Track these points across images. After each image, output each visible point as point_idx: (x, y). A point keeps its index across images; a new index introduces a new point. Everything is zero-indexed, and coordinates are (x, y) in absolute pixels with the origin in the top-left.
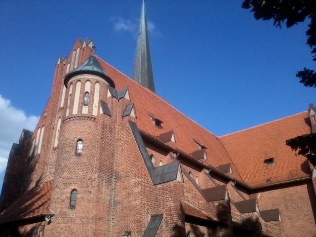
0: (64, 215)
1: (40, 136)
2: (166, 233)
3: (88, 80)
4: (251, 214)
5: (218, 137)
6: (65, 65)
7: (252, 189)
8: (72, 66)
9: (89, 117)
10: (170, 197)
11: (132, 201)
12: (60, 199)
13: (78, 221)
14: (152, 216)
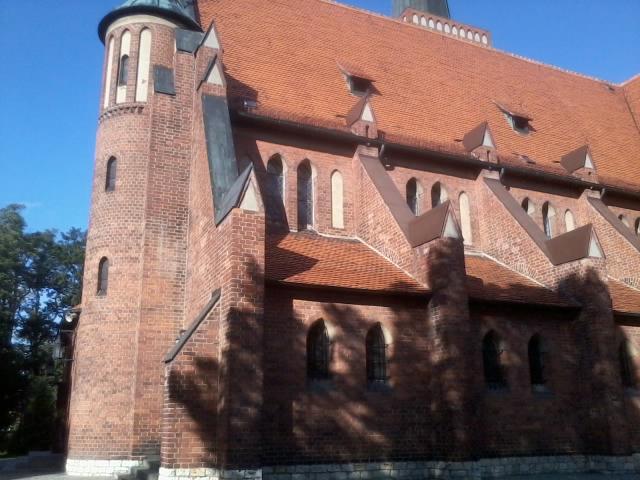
4: (576, 264)
9: (128, 108)
13: (112, 317)
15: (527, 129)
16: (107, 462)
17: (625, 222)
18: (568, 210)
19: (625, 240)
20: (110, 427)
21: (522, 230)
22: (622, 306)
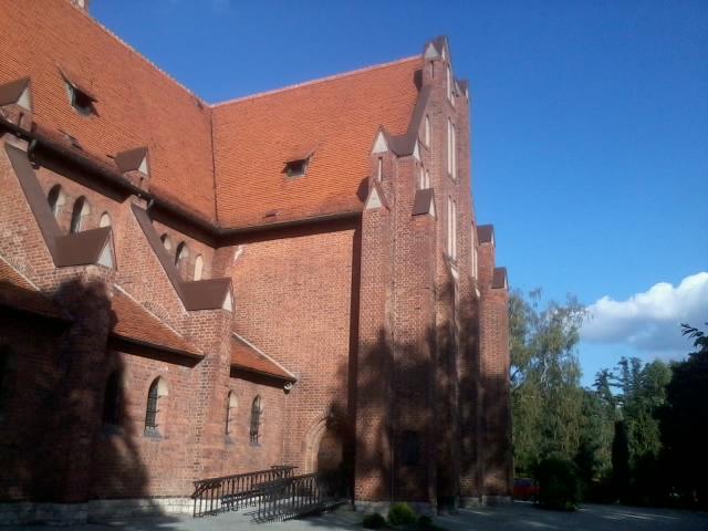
4: (80, 269)
5: (204, 103)
7: (221, 232)
15: (88, 109)
17: (168, 246)
18: (105, 213)
19: (157, 259)
21: (32, 218)
22: (124, 330)
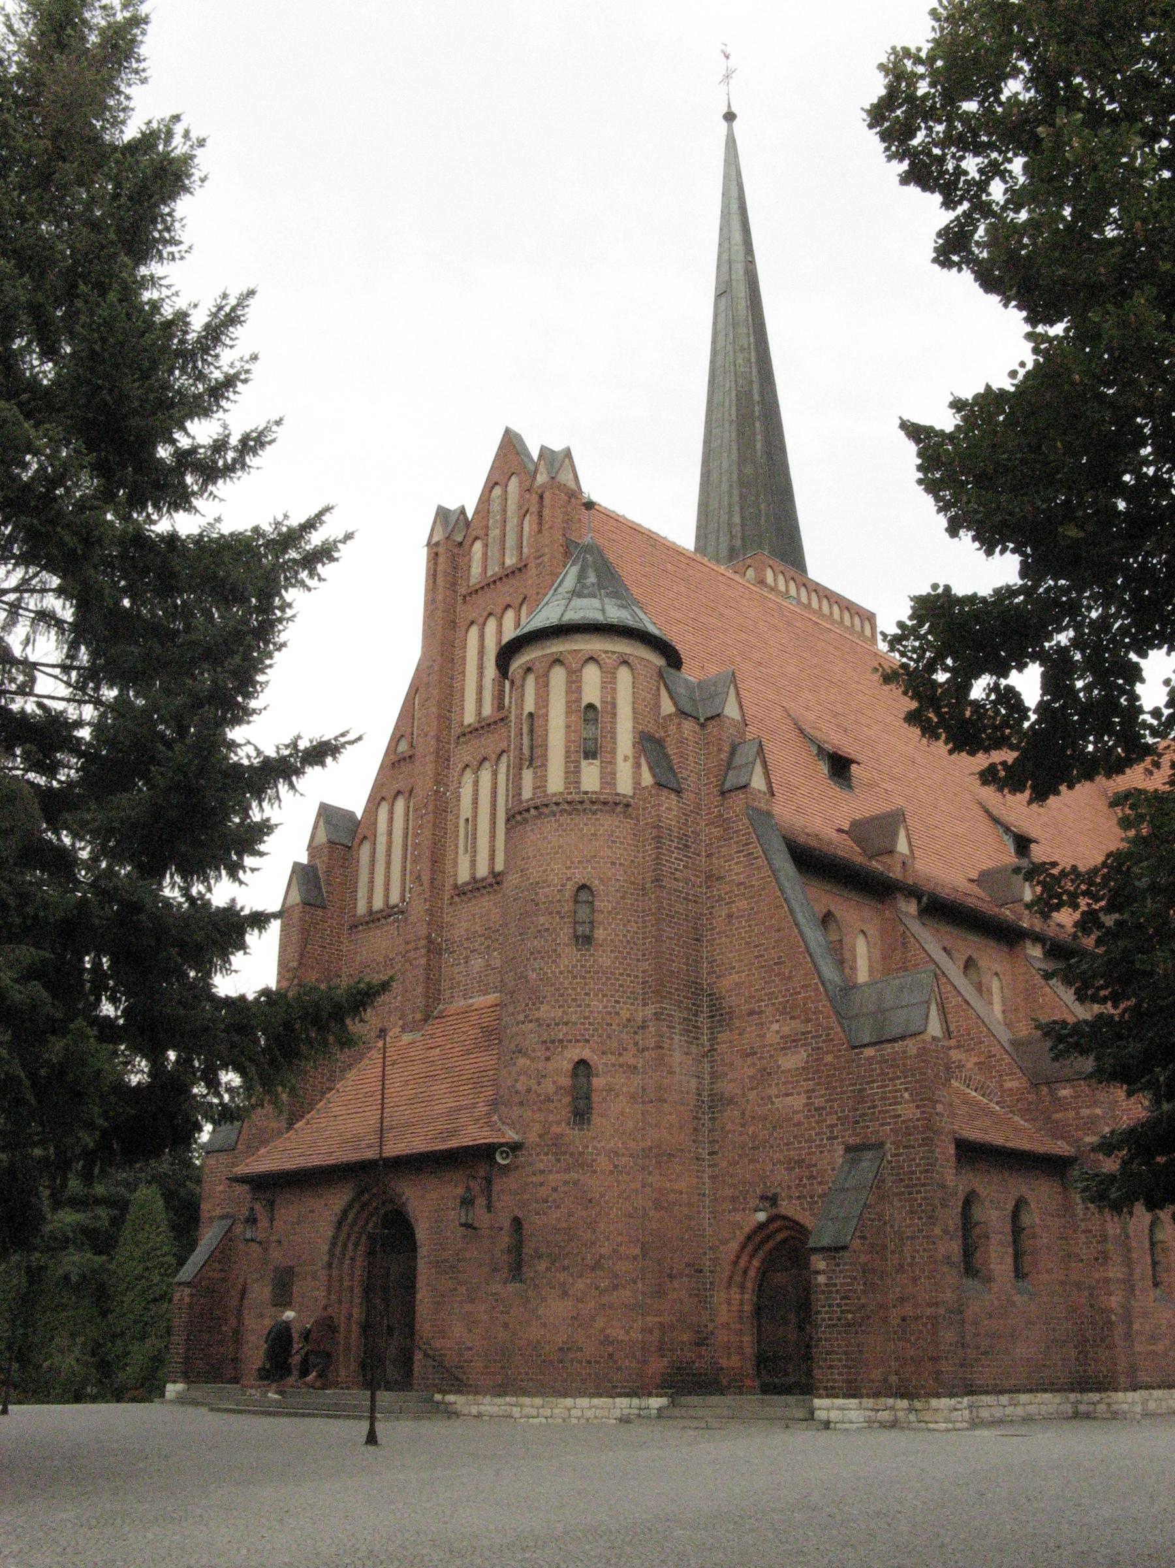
0: (556, 1146)
1: (390, 833)
2: (897, 1204)
3: (591, 659)
6: (460, 544)
8: (493, 551)
10: (906, 1089)
11: (777, 1096)
12: (538, 1095)
14: (849, 1149)
16: (610, 1400)
20: (611, 1343)
